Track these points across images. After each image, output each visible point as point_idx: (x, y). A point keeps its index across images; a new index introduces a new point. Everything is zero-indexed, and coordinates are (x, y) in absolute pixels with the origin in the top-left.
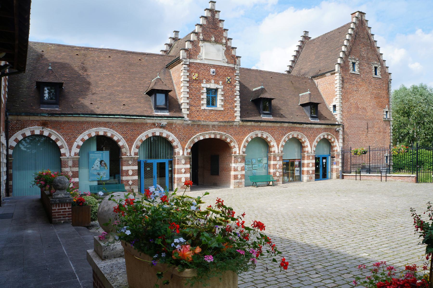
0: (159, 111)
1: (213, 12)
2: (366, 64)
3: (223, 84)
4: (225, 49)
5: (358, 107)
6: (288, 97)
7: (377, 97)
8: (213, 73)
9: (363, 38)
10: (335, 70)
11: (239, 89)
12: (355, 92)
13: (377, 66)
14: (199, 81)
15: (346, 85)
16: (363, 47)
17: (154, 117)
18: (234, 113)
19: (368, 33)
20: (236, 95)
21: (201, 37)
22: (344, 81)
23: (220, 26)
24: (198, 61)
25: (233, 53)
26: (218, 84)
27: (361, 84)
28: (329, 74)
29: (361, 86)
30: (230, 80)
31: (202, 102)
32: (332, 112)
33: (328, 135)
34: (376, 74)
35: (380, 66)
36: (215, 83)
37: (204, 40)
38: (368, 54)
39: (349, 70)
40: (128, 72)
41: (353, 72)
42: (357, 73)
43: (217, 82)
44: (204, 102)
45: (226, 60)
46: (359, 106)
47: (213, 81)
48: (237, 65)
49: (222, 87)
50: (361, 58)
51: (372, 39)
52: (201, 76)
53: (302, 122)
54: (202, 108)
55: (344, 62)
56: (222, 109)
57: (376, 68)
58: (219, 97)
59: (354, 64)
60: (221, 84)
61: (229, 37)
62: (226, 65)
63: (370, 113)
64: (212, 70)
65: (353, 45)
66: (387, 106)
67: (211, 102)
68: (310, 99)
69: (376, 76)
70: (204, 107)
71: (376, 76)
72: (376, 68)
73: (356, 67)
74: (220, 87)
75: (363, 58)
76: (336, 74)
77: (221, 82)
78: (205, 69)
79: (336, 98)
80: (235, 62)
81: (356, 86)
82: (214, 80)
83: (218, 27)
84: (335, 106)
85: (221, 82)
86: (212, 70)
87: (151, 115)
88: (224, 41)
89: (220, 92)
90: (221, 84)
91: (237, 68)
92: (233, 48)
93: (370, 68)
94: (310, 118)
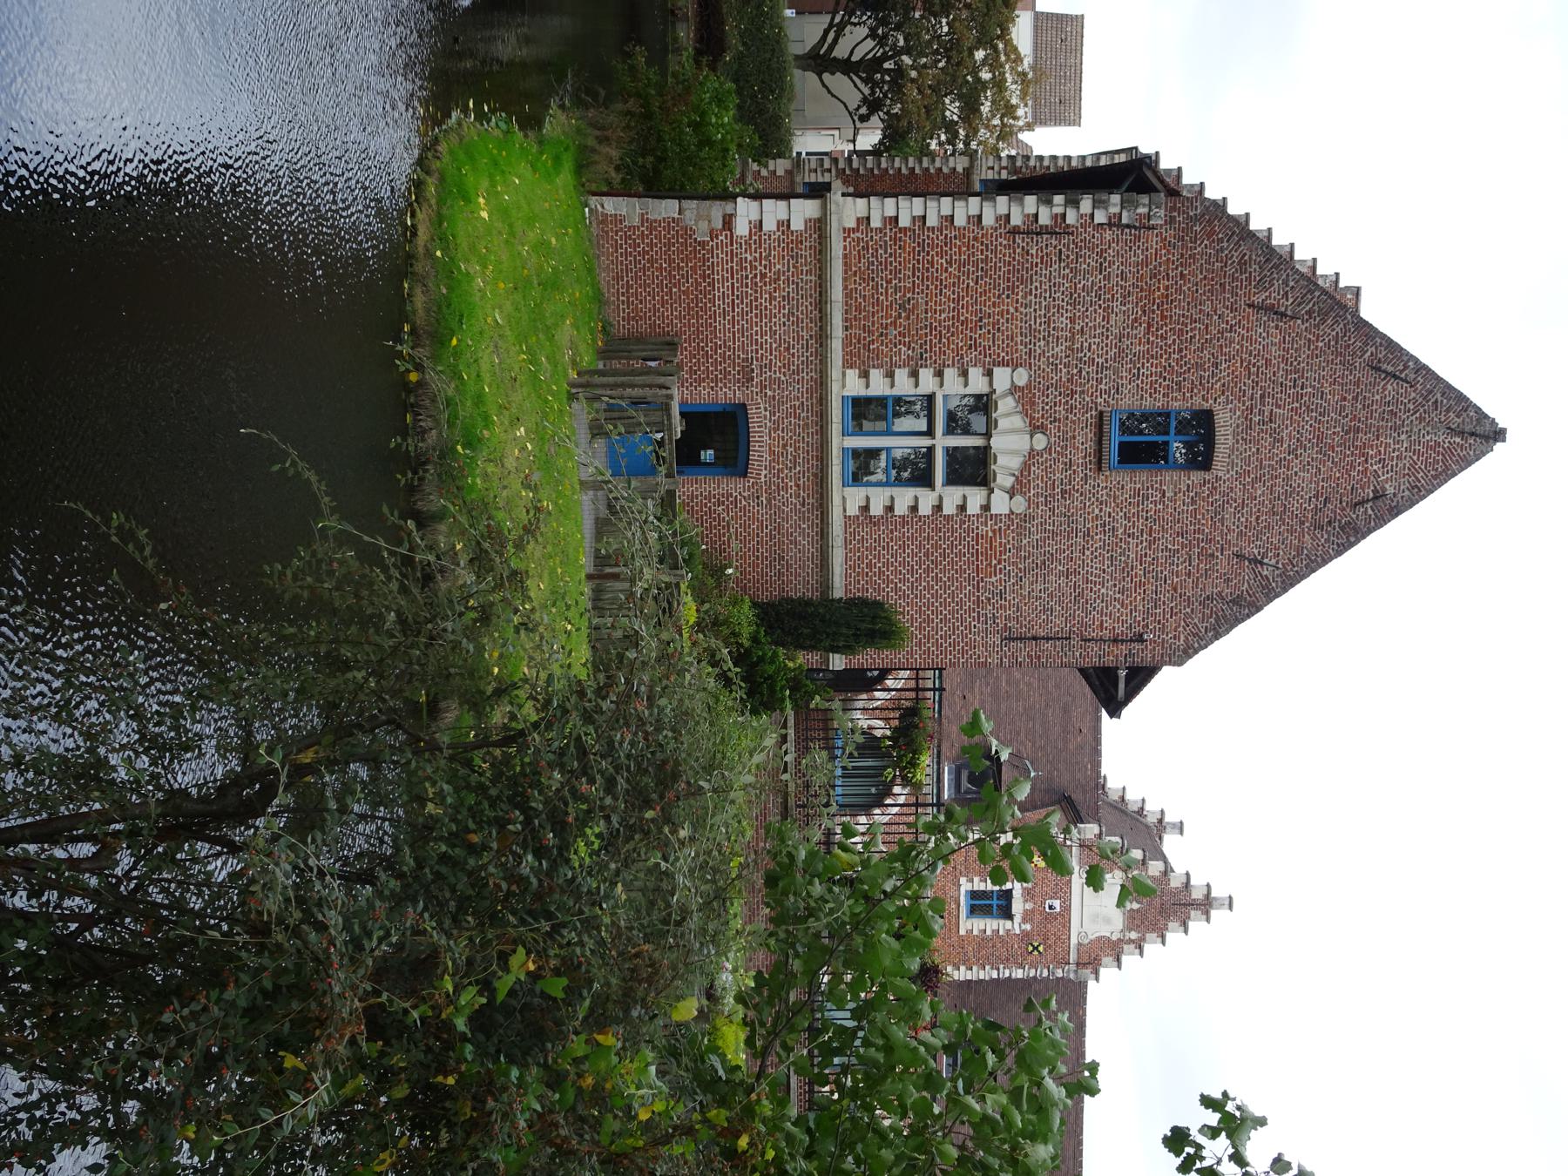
0: (953, 776)
1: (1206, 905)
3: (1025, 934)
4: (1114, 938)
8: (1051, 907)
11: (1013, 976)
17: (938, 763)
18: (954, 965)
20: (998, 969)
23: (1170, 924)
25: (1106, 960)
26: (1024, 920)
30: (1036, 953)
31: (976, 879)
36: (1026, 911)
40: (1047, 705)
44: (979, 885)
45: (1086, 941)
47: (1029, 906)
48: (1076, 972)
49: (1018, 932)
54: (963, 880)
56: (962, 932)
58: (990, 925)
60: (1023, 927)
61: (1147, 947)
62: (1074, 941)
70: (965, 886)
74: (1016, 926)
77: (1028, 927)
78: (1057, 885)
80: (1085, 965)
82: (1033, 911)
83: (1167, 918)
85: (1028, 927)
86: (1057, 903)
87: (943, 757)
88: (1133, 935)
89: (1003, 925)
90: (1023, 927)
91: (1068, 971)
92: (1118, 960)
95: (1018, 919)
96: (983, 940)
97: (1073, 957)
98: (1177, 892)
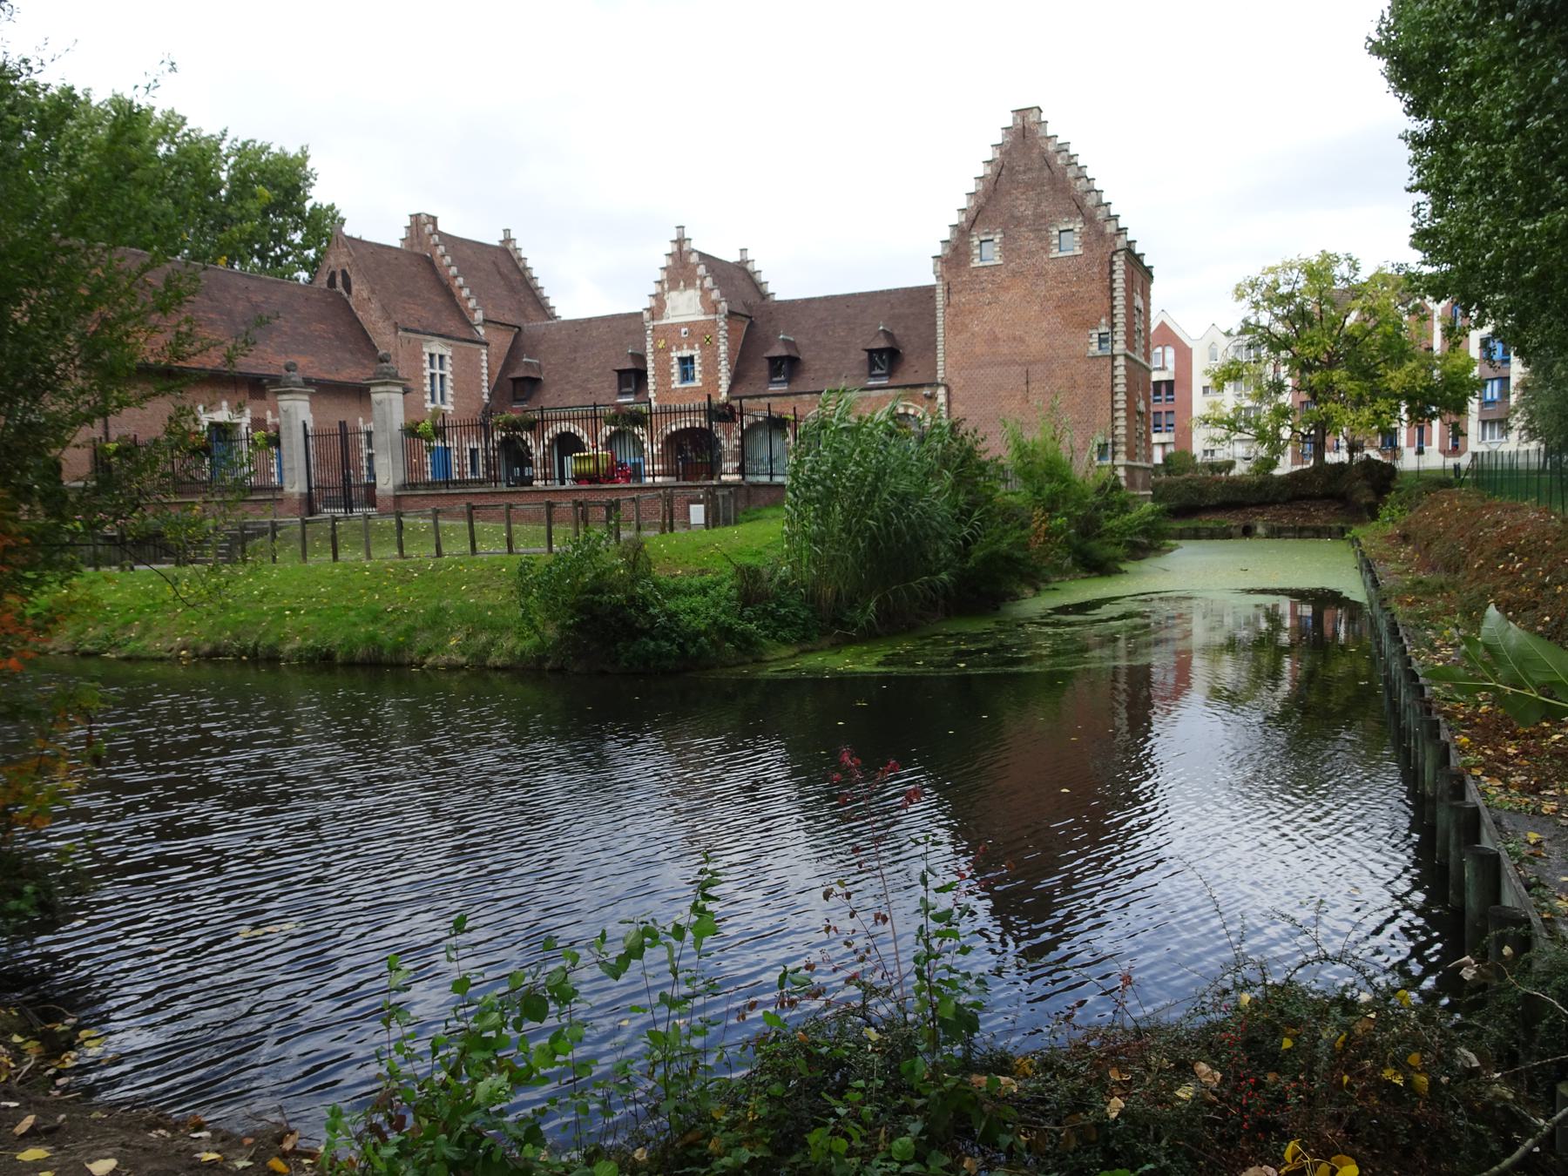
3: (702, 347)
5: (996, 339)
12: (987, 308)
14: (668, 350)
15: (954, 299)
16: (1023, 193)
21: (666, 286)
24: (664, 322)
26: (693, 348)
27: (1005, 284)
29: (1007, 289)
33: (907, 407)
37: (670, 289)
43: (691, 347)
52: (669, 343)
62: (703, 318)
63: (1036, 344)
64: (683, 330)
65: (989, 199)
66: (1103, 321)
67: (686, 376)
70: (676, 385)
74: (696, 353)
75: (1019, 221)
81: (992, 293)
83: (689, 263)
88: (698, 282)
89: (697, 361)
95: (693, 353)
96: (705, 372)
97: (712, 317)
98: (675, 261)
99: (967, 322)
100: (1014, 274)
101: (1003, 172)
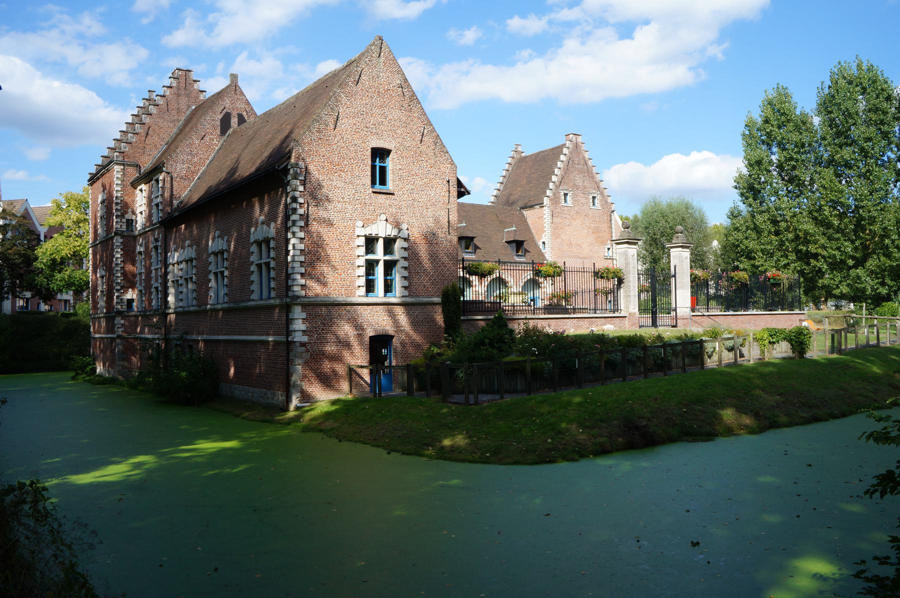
2: (581, 195)
5: (571, 244)
6: (492, 233)
7: (596, 231)
9: (579, 164)
10: (543, 203)
13: (596, 195)
16: (578, 174)
19: (584, 158)
22: (554, 215)
27: (574, 217)
28: (538, 207)
29: (575, 219)
32: (542, 249)
34: (594, 204)
35: (599, 196)
38: (584, 182)
39: (560, 203)
41: (565, 205)
42: (569, 206)
46: (572, 242)
50: (576, 187)
51: (590, 164)
53: (506, 261)
55: (554, 194)
57: (594, 198)
59: (566, 195)
65: (565, 173)
68: (515, 237)
69: (594, 208)
71: (594, 208)
72: (594, 198)
73: (568, 198)
76: (545, 208)
79: (545, 234)
84: (544, 243)
93: (587, 198)
94: (515, 257)
99: (560, 233)
100: (577, 213)
101: (570, 162)
